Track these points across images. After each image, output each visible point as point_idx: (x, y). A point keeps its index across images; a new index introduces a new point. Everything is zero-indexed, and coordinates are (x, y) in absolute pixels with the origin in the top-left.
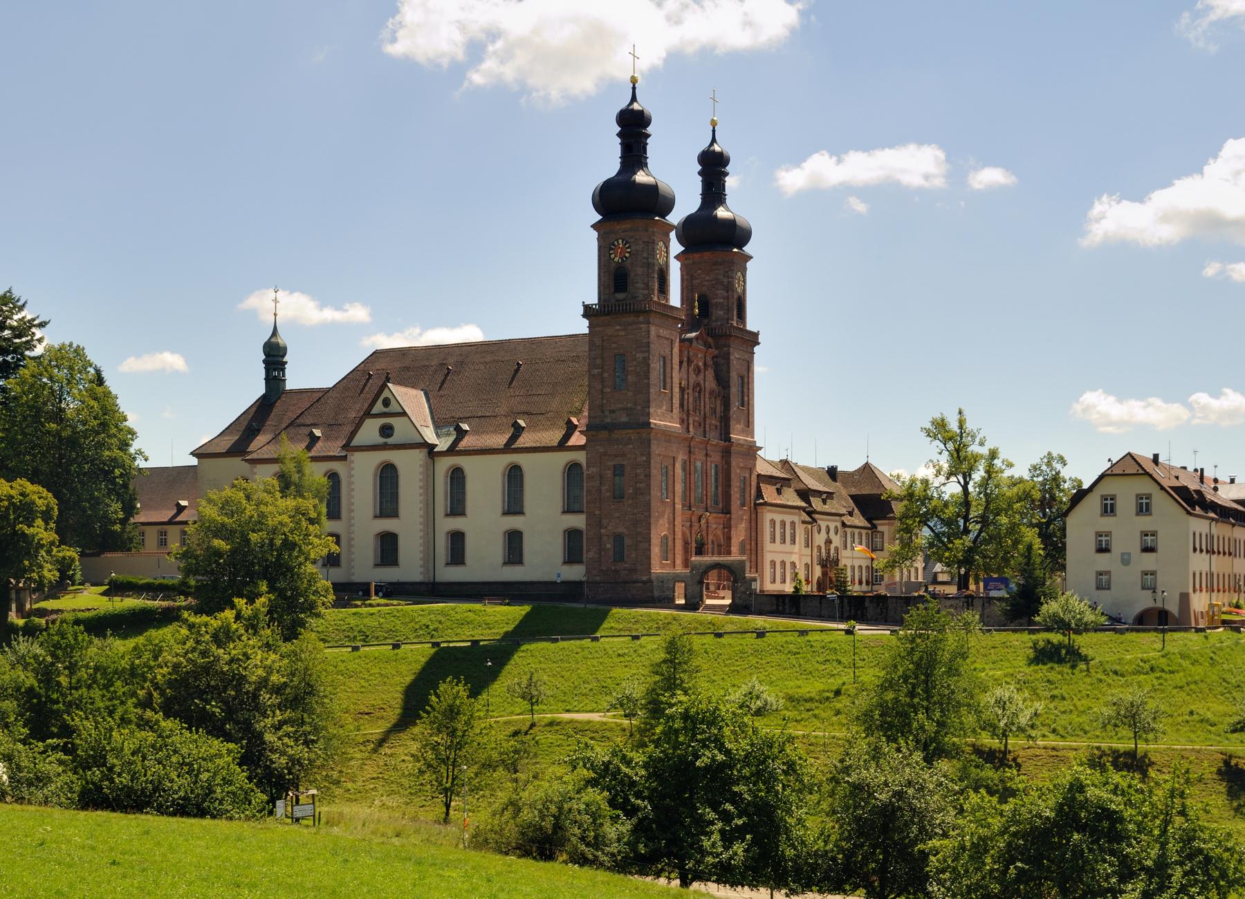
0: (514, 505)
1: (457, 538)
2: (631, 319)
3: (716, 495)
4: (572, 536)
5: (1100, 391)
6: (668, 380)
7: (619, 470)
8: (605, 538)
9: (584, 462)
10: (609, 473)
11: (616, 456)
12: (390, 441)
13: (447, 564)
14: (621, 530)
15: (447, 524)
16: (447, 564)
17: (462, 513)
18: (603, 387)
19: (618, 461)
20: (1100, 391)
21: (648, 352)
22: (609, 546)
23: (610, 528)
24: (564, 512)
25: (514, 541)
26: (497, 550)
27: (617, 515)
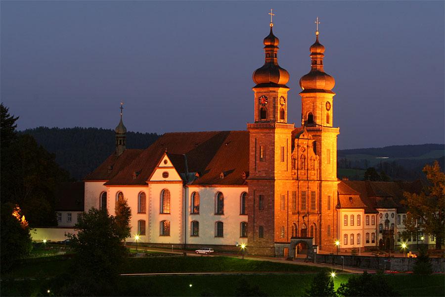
0: (220, 210)
1: (196, 224)
2: (267, 131)
3: (191, 206)
4: (243, 224)
5: (21, 126)
6: (285, 157)
7: (261, 198)
8: (255, 227)
9: (238, 191)
10: (257, 199)
11: (260, 191)
12: (167, 179)
13: (215, 237)
14: (262, 224)
15: (221, 218)
16: (215, 237)
17: (222, 214)
18: (256, 160)
19: (261, 193)
20: (21, 126)
21: (274, 146)
22: (257, 231)
23: (258, 223)
24: (240, 214)
25: (220, 226)
26: (213, 232)
27: (261, 217)
